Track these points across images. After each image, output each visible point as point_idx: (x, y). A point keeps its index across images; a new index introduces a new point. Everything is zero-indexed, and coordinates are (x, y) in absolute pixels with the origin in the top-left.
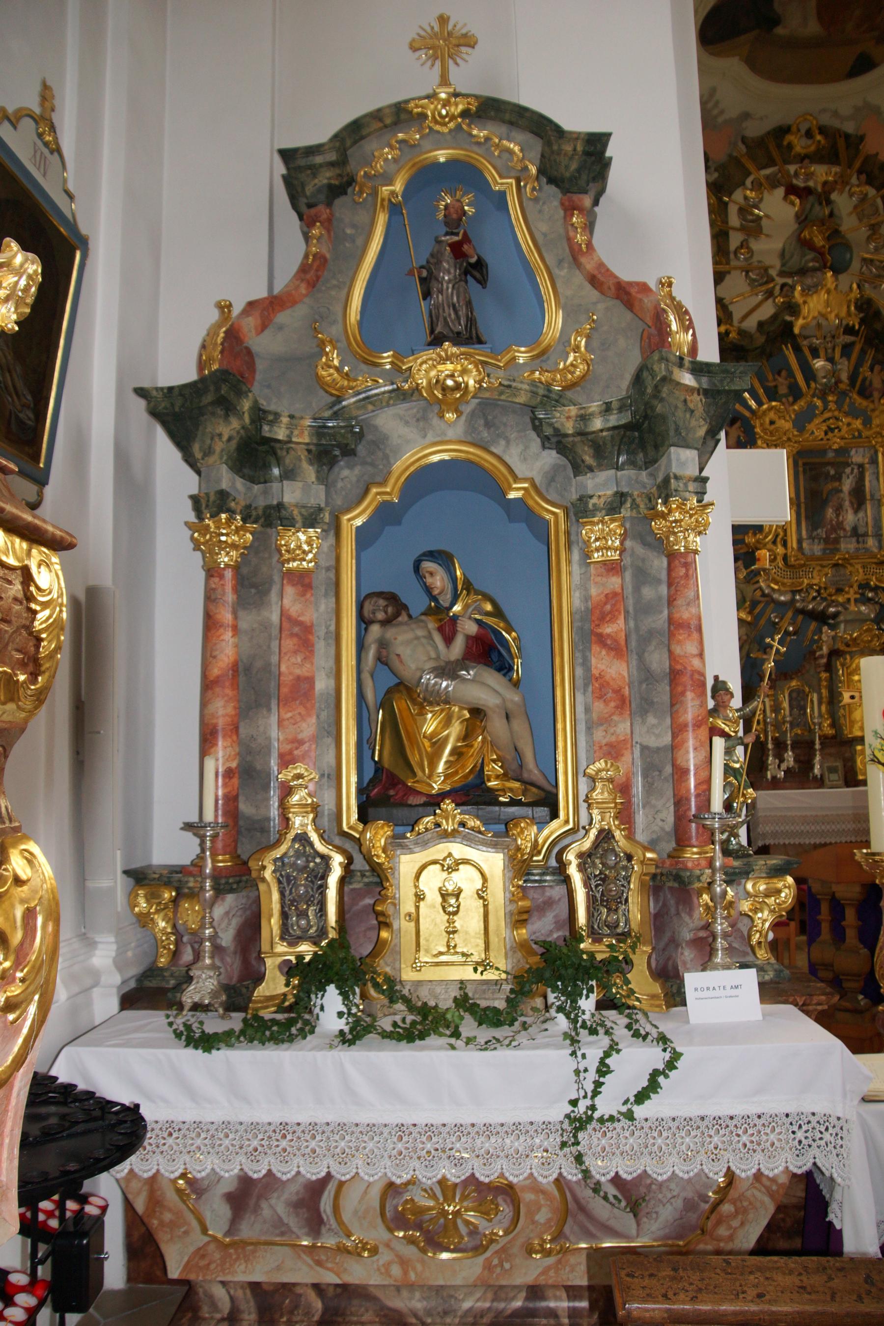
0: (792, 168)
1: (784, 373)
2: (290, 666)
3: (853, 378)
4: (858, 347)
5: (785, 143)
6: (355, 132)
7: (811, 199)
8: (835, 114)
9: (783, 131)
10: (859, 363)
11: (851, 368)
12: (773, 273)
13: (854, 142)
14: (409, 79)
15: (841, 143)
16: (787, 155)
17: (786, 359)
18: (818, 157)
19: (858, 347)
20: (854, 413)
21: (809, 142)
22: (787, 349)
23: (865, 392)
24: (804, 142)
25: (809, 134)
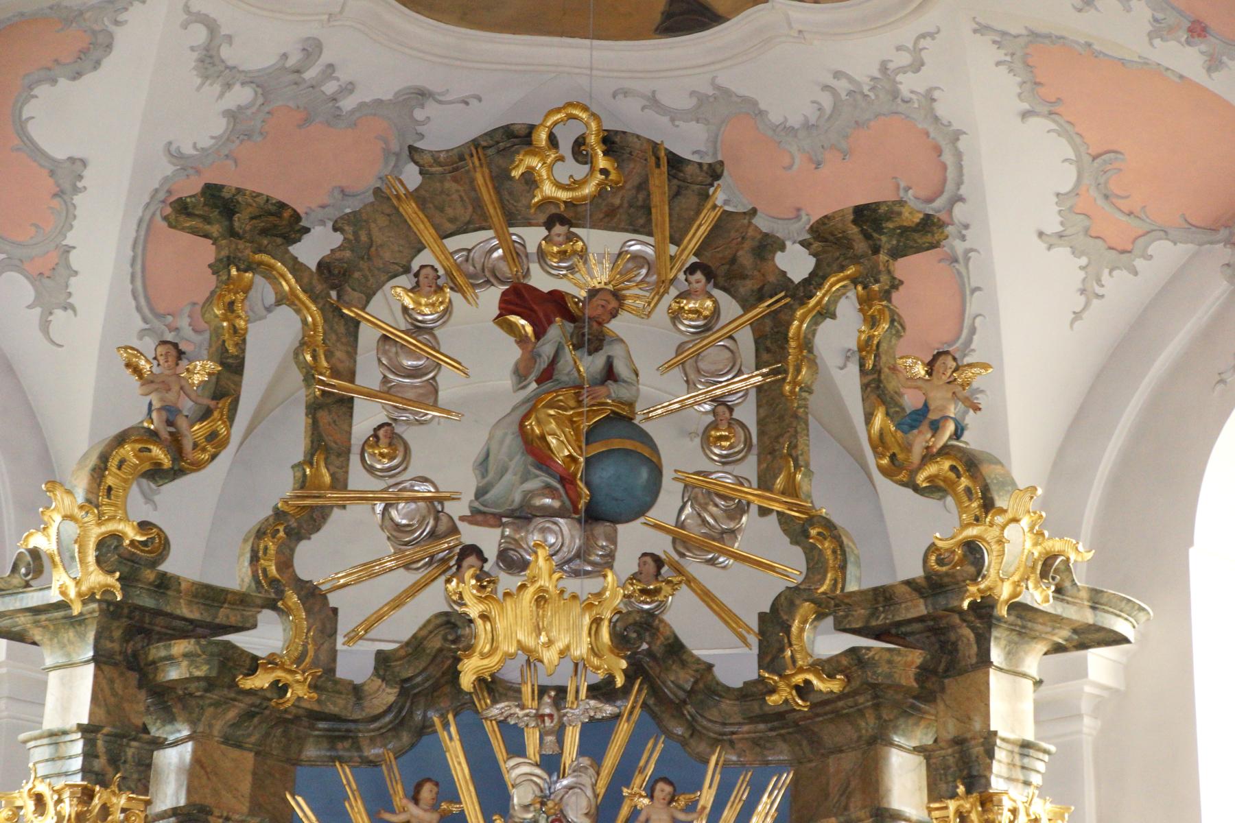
0: (533, 236)
1: (427, 792)
4: (623, 730)
5: (516, 174)
7: (557, 331)
8: (653, 102)
9: (516, 138)
10: (623, 775)
11: (601, 789)
12: (457, 509)
13: (690, 179)
17: (441, 753)
18: (604, 212)
19: (623, 730)
21: (581, 171)
22: (446, 725)
24: (571, 169)
25: (580, 149)
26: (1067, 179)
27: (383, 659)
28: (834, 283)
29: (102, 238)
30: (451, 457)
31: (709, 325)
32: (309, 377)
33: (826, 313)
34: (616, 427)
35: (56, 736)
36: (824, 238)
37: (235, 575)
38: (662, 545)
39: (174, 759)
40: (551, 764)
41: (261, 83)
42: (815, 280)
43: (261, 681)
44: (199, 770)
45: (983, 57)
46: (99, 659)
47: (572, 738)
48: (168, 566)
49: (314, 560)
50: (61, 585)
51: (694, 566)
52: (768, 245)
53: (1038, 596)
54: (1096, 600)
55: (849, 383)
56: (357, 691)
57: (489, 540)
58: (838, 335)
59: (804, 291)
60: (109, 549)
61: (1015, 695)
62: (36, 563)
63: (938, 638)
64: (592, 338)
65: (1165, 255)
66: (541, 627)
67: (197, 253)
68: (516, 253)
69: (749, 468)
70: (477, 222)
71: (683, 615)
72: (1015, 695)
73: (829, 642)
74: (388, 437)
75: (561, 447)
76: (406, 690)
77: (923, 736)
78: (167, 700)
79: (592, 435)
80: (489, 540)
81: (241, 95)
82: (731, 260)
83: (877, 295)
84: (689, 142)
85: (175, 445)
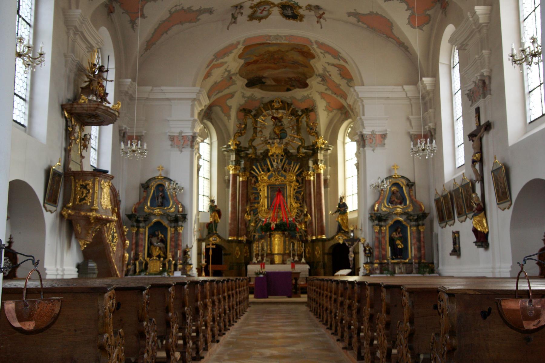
0: (274, 111)
2: (140, 243)
3: (283, 167)
6: (150, 180)
7: (277, 121)
8: (286, 97)
9: (272, 102)
12: (268, 138)
13: (289, 105)
14: (156, 175)
15: (286, 105)
16: (272, 108)
18: (281, 108)
20: (282, 176)
23: (285, 171)
24: (278, 104)
26: (325, 105)
27: (261, 153)
28: (304, 115)
29: (233, 113)
30: (267, 133)
31: (291, 119)
32: (253, 126)
33: (303, 118)
34: (283, 131)
35: (232, 161)
36: (303, 111)
37: (247, 146)
38: (287, 141)
39: (243, 163)
40: (277, 163)
41: (248, 98)
42: (302, 115)
43: (250, 156)
44: (245, 164)
45: (317, 94)
46: (236, 154)
47: (279, 160)
48: (241, 145)
49: (254, 144)
50: (232, 147)
51: (290, 143)
52: (297, 111)
53: (323, 146)
54: (328, 146)
55: (305, 123)
56: (259, 156)
57: (271, 141)
58: (304, 120)
59: (300, 116)
60: (236, 144)
61: (321, 156)
62: (230, 146)
63: (314, 150)
64: (280, 121)
65: (335, 111)
66: (275, 149)
67: (242, 114)
68: (273, 113)
69: (296, 133)
70: (269, 110)
71: (289, 148)
72: (321, 156)
73: (305, 151)
74: (261, 131)
75: (278, 132)
76: (263, 156)
77: (312, 159)
78: (241, 158)
79: (280, 131)
80: (271, 141)
81: (246, 99)
82: (294, 113)
83: (308, 116)
84: (289, 101)
85: (241, 133)
